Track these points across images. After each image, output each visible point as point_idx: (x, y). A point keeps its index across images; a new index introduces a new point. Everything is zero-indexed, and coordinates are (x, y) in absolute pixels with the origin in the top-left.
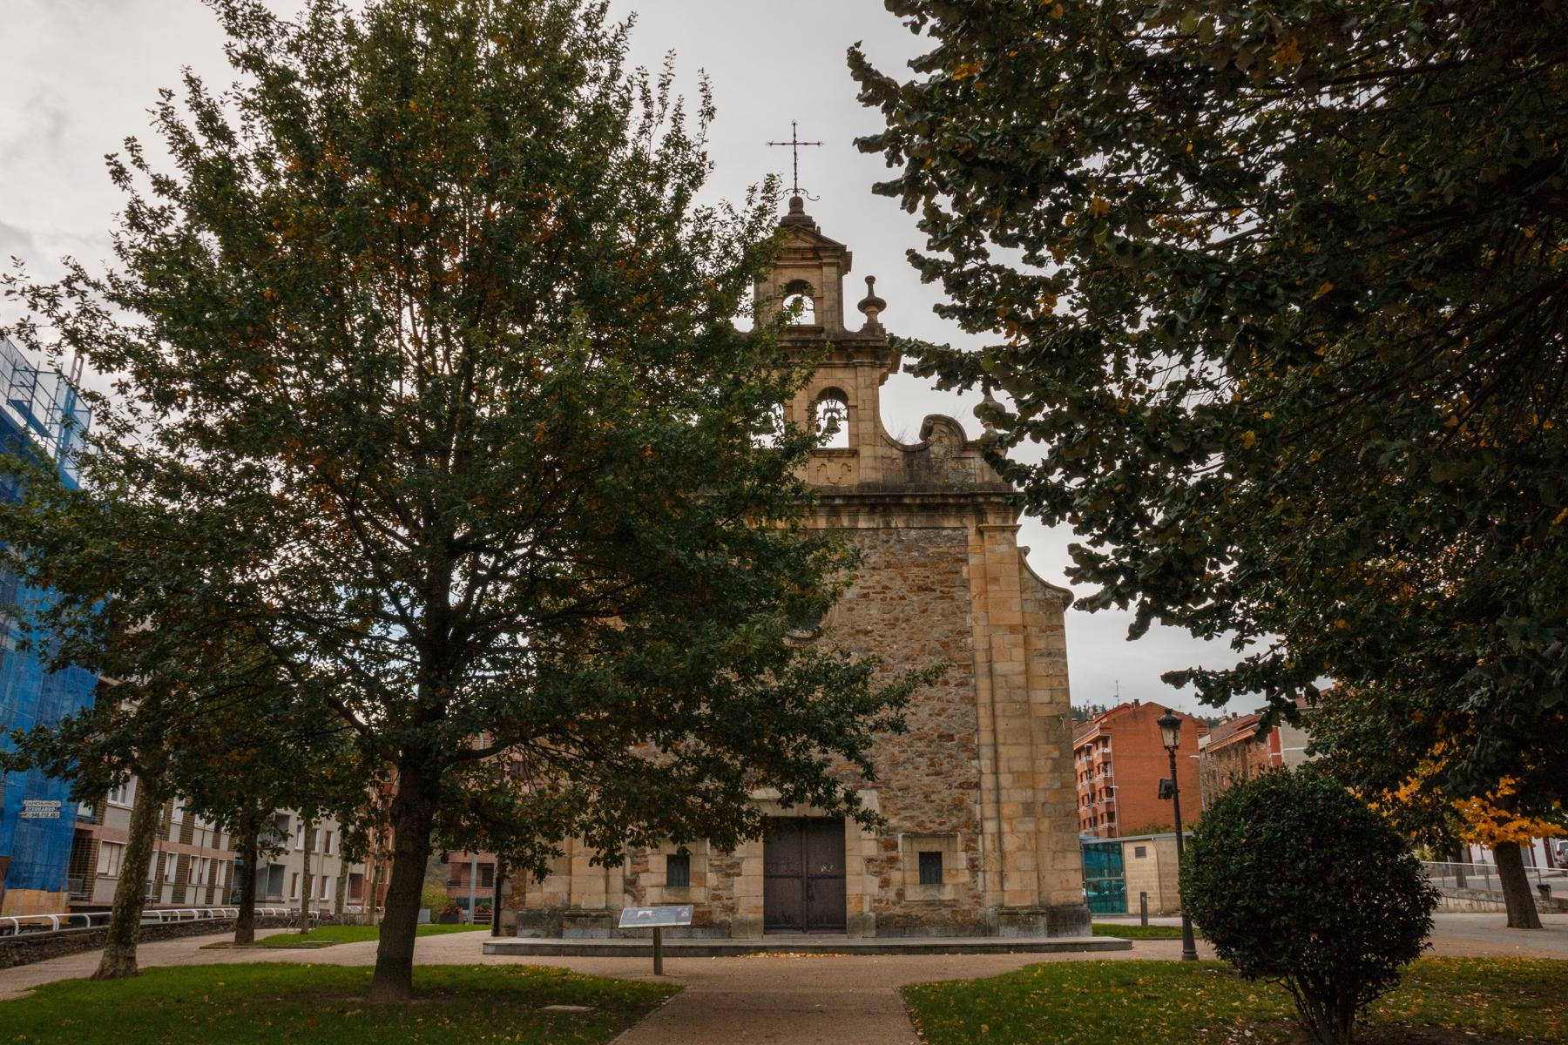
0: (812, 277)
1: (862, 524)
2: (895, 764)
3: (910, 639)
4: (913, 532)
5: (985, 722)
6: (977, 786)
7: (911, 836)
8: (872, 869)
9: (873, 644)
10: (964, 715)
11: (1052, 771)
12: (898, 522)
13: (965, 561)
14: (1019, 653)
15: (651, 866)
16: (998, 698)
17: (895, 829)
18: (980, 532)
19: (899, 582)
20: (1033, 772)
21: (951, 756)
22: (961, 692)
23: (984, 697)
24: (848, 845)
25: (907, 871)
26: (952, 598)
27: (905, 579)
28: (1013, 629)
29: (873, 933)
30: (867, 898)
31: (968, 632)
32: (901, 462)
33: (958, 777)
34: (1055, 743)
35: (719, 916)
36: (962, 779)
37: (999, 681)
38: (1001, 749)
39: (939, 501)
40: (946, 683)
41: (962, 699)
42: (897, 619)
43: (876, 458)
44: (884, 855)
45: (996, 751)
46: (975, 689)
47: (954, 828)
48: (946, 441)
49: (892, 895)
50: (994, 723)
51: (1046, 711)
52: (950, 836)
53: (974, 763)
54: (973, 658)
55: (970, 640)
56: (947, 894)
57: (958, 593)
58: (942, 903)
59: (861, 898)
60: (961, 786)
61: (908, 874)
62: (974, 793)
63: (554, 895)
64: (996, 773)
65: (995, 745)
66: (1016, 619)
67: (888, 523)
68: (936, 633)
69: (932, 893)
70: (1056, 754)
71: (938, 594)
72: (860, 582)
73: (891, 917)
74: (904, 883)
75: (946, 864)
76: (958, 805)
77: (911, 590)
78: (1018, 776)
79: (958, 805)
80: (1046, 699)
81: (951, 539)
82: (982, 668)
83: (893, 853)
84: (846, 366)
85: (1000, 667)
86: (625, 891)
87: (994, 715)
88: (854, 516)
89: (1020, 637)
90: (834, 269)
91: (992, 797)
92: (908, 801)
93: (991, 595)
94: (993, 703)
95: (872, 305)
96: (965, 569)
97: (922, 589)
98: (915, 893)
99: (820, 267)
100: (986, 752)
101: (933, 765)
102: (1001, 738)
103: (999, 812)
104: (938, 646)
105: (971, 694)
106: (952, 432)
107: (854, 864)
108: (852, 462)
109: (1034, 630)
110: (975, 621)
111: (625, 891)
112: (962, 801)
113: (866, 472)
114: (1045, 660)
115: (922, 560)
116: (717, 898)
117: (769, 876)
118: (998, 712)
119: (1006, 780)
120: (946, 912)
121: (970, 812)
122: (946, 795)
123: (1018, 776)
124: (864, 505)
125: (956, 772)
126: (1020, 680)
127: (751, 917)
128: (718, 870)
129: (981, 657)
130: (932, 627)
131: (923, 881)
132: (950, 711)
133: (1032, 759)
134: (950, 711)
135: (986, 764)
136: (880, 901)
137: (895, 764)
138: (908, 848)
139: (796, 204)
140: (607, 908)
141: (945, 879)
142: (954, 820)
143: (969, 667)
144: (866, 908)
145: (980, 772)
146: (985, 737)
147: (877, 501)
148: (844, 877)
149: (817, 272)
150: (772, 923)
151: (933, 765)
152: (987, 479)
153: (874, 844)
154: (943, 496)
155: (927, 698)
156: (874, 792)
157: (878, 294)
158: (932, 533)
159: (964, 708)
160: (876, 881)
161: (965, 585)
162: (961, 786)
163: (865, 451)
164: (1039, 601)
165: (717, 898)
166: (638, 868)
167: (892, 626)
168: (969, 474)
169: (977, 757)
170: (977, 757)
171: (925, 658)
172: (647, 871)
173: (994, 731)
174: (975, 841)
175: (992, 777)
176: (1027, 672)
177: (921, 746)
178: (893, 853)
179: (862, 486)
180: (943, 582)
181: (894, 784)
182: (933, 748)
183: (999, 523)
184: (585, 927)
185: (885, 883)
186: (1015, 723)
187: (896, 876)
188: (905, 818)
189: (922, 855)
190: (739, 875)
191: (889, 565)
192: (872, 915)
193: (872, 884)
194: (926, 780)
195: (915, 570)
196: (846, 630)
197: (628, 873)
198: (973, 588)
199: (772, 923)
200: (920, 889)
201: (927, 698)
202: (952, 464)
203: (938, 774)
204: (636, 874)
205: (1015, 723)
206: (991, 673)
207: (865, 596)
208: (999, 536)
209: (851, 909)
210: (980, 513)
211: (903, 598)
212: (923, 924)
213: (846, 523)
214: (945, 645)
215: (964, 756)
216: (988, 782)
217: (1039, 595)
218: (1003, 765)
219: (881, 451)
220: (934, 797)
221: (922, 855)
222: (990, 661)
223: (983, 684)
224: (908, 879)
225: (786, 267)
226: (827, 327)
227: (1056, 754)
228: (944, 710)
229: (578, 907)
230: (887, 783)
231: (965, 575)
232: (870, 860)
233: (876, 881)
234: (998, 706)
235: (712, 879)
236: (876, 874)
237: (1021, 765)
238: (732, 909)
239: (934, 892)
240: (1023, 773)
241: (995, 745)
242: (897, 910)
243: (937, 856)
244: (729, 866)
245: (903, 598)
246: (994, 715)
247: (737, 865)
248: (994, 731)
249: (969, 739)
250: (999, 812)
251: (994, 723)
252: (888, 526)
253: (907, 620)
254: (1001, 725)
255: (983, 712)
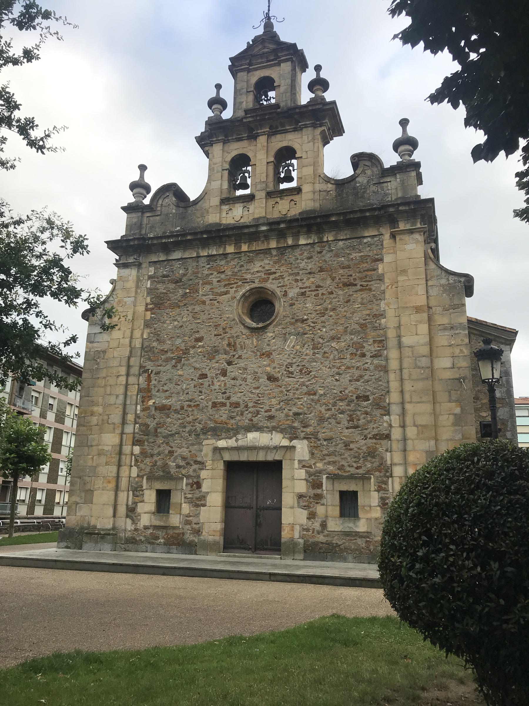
0: (273, 73)
1: (302, 241)
2: (321, 420)
3: (336, 323)
4: (341, 243)
5: (394, 385)
6: (388, 437)
7: (333, 478)
8: (302, 504)
9: (307, 328)
10: (378, 380)
11: (455, 424)
12: (329, 237)
13: (381, 260)
14: (424, 328)
15: (146, 498)
16: (405, 365)
17: (320, 472)
18: (393, 236)
19: (329, 282)
20: (436, 426)
21: (366, 413)
22: (376, 361)
23: (394, 365)
24: (285, 483)
25: (330, 507)
26: (370, 290)
27: (333, 279)
28: (418, 309)
29: (302, 556)
30: (297, 528)
31: (382, 315)
32: (333, 193)
33: (372, 429)
34: (457, 401)
35: (189, 537)
36: (375, 431)
37: (407, 352)
38: (408, 406)
39: (358, 215)
40: (363, 355)
41: (376, 367)
42: (326, 309)
43: (314, 192)
44: (312, 492)
45: (403, 409)
46: (387, 360)
47: (368, 472)
48: (369, 172)
49: (317, 526)
50: (402, 385)
51: (448, 375)
52: (364, 478)
53: (386, 418)
54: (385, 335)
55: (383, 321)
56: (361, 526)
57: (374, 285)
58: (357, 534)
59: (292, 526)
60: (374, 437)
61: (330, 508)
62: (384, 442)
63: (83, 517)
64: (403, 426)
65: (403, 403)
66: (422, 301)
67: (322, 238)
68: (356, 317)
69: (349, 525)
70: (458, 410)
71: (359, 287)
72: (300, 284)
73: (316, 544)
74: (326, 517)
75: (361, 501)
76: (372, 453)
77: (338, 287)
78: (422, 428)
79: (372, 453)
80: (449, 364)
81: (370, 245)
82: (392, 342)
83: (319, 491)
84: (295, 130)
85: (406, 341)
86: (127, 516)
87: (402, 380)
88: (296, 236)
89: (425, 316)
90: (289, 63)
91: (401, 446)
92: (331, 449)
93: (400, 284)
94: (401, 370)
95: (319, 84)
96: (381, 268)
97: (346, 285)
98: (335, 525)
99: (279, 64)
100: (395, 409)
101: (352, 420)
102: (407, 397)
103: (405, 458)
104: (357, 327)
105: (383, 363)
106: (373, 164)
107: (288, 499)
108: (296, 198)
109: (439, 310)
110: (388, 306)
111: (127, 516)
112: (376, 449)
113: (306, 203)
114: (447, 333)
115: (346, 263)
116: (188, 523)
117: (228, 506)
118: (405, 376)
119: (411, 432)
120: (361, 542)
121: (382, 458)
122: (362, 444)
123: (422, 428)
124: (302, 226)
125: (371, 425)
126: (425, 350)
127: (211, 538)
128: (190, 501)
129: (391, 334)
130: (353, 313)
131: (342, 515)
132: (366, 377)
133: (435, 414)
134: (366, 377)
135: (395, 419)
136: (307, 530)
137: (321, 420)
138: (330, 487)
139: (268, 26)
140: (114, 528)
141: (361, 514)
142: (369, 465)
143: (382, 342)
144: (297, 535)
145: (390, 426)
146: (394, 397)
147: (312, 223)
148: (280, 509)
149: (276, 69)
150: (231, 542)
151: (352, 420)
152: (400, 195)
153: (304, 483)
154: (361, 211)
155: (349, 368)
156: (305, 442)
157: (323, 75)
158: (355, 242)
159: (377, 374)
160: (305, 513)
161: (381, 278)
162: (374, 437)
163: (306, 188)
164: (443, 286)
165: (188, 523)
166: (137, 499)
167: (323, 314)
168: (386, 195)
169: (388, 414)
170: (388, 414)
171: (348, 337)
172: (142, 501)
173: (402, 392)
174: (386, 483)
175: (400, 430)
176: (431, 342)
177: (342, 405)
178: (319, 491)
179: (300, 214)
180: (364, 279)
181: (320, 435)
182: (352, 406)
183: (408, 227)
184: (96, 542)
185: (312, 516)
186: (420, 385)
187: (320, 510)
188: (329, 463)
189: (342, 494)
190: (204, 505)
191: (321, 270)
192: (301, 541)
193: (302, 516)
194: (347, 432)
195: (341, 271)
196: (288, 320)
197: (130, 503)
198: (386, 280)
199: (231, 542)
200: (339, 521)
201: (349, 368)
202: (374, 188)
203: (356, 427)
204: (135, 503)
205: (420, 385)
206: (400, 345)
207: (303, 294)
208: (406, 237)
209: (285, 535)
210: (393, 221)
211: (331, 293)
212: (342, 551)
213: (290, 242)
214: (363, 326)
215: (377, 412)
216: (396, 434)
217: (443, 281)
218: (409, 420)
219: (318, 187)
220: (352, 446)
221: (342, 494)
222: (399, 337)
223: (393, 354)
224: (330, 513)
225: (256, 69)
226: (282, 105)
227: (458, 410)
228: (361, 376)
229: (95, 527)
230: (315, 435)
231: (380, 271)
232: (300, 496)
233: (305, 513)
234: (404, 371)
235: (186, 508)
236: (305, 507)
237: (425, 420)
238: (198, 532)
239: (351, 525)
240: (425, 426)
241: (403, 403)
242: (321, 538)
243: (354, 495)
244: (199, 499)
245: (331, 293)
246: (402, 380)
247: (203, 497)
248: (402, 392)
249: (382, 398)
250: (405, 458)
251: (402, 385)
252: (321, 242)
253: (334, 309)
254: (408, 386)
255: (392, 376)
